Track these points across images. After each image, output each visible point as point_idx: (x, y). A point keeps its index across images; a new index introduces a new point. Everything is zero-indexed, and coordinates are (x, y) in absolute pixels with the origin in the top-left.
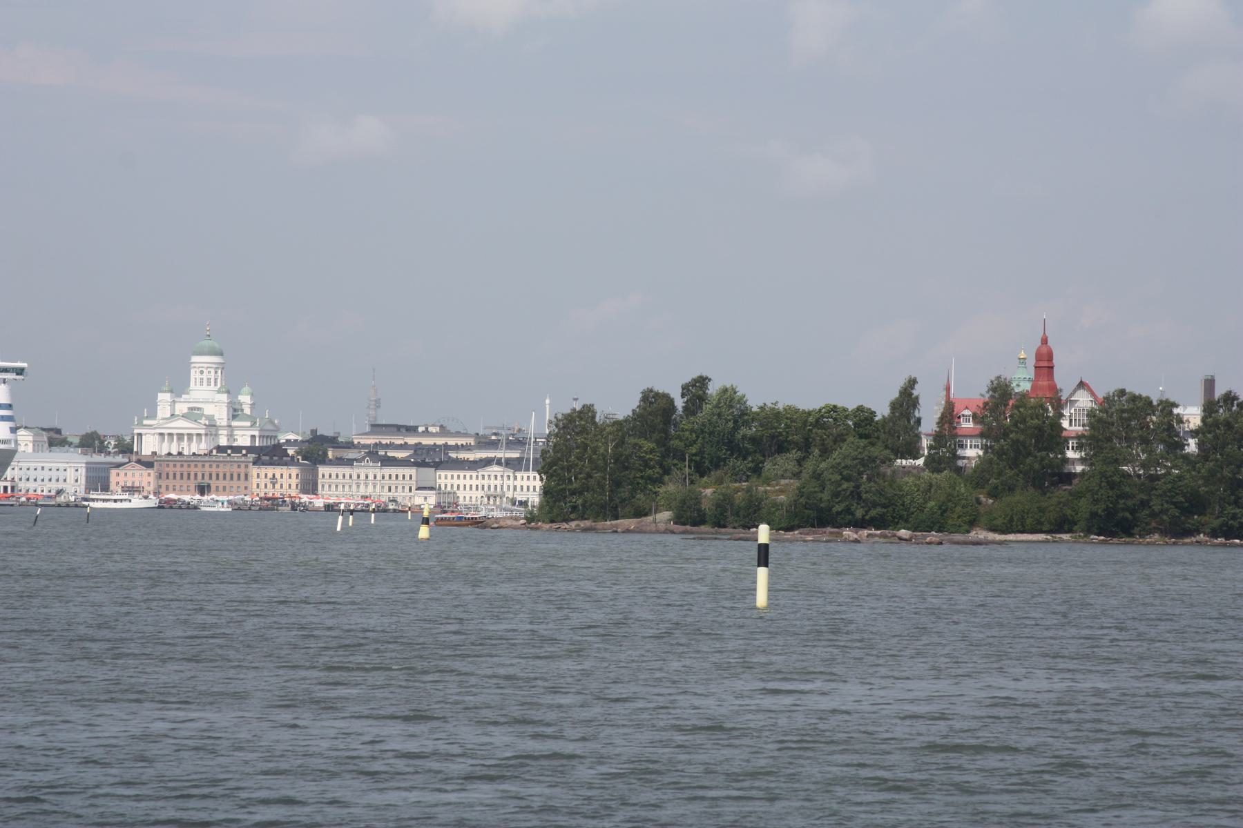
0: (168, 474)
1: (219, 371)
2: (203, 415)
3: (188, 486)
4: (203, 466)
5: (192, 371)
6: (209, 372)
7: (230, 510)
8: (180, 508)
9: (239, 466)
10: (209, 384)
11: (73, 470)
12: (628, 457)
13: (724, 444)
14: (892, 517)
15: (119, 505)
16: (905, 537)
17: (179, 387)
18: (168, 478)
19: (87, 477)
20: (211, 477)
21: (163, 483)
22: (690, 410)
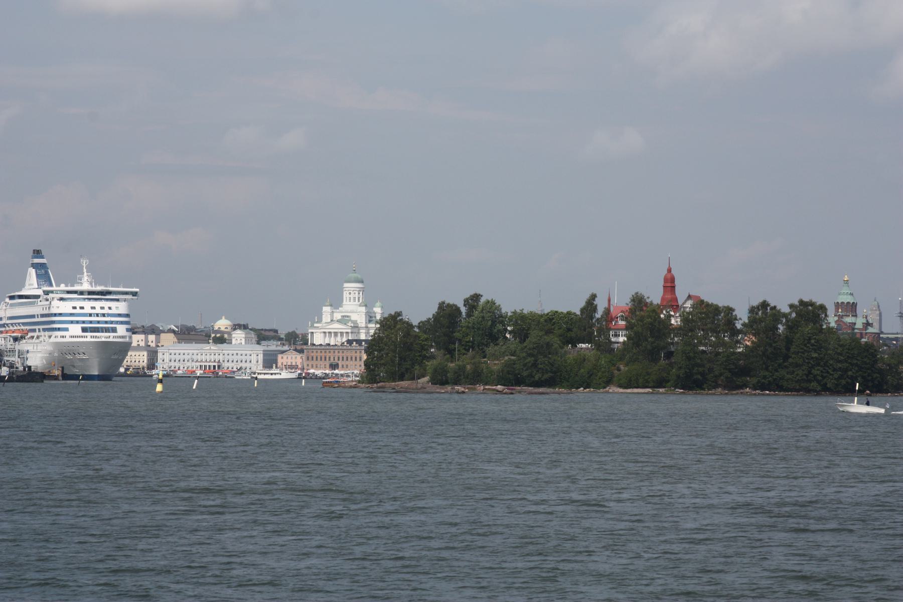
0: (313, 357)
1: (361, 293)
2: (350, 320)
3: (325, 365)
4: (334, 352)
5: (345, 293)
6: (355, 293)
7: (250, 378)
8: (311, 378)
9: (356, 352)
10: (354, 300)
11: (255, 355)
12: (412, 344)
13: (486, 335)
14: (560, 378)
15: (274, 377)
16: (500, 390)
17: (336, 303)
18: (312, 359)
19: (264, 360)
20: (339, 360)
21: (310, 363)
22: (469, 315)
